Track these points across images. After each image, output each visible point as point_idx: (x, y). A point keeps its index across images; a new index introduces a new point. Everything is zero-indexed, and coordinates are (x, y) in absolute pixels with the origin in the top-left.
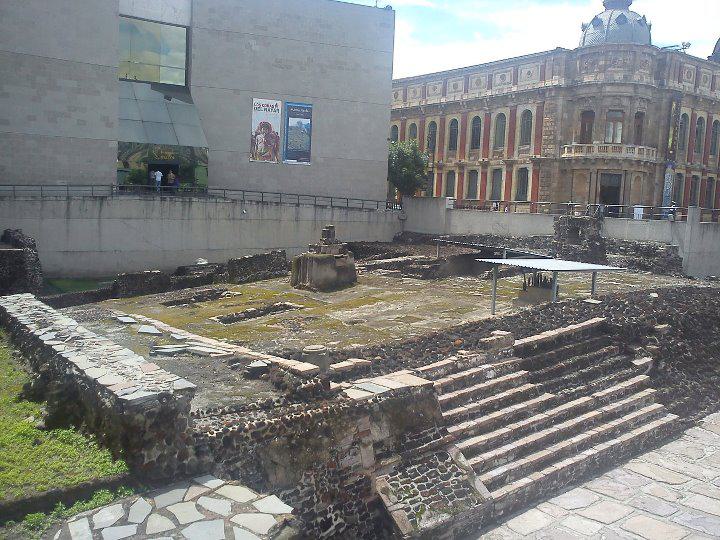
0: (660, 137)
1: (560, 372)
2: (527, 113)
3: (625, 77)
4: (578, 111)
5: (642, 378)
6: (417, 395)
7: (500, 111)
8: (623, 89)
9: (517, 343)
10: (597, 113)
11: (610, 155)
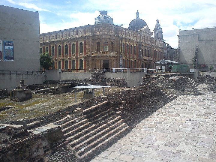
0: (118, 49)
1: (97, 118)
2: (81, 43)
3: (108, 33)
4: (95, 42)
5: (119, 117)
6: (56, 130)
7: (73, 43)
8: (107, 36)
9: (84, 111)
10: (101, 44)
11: (105, 55)
